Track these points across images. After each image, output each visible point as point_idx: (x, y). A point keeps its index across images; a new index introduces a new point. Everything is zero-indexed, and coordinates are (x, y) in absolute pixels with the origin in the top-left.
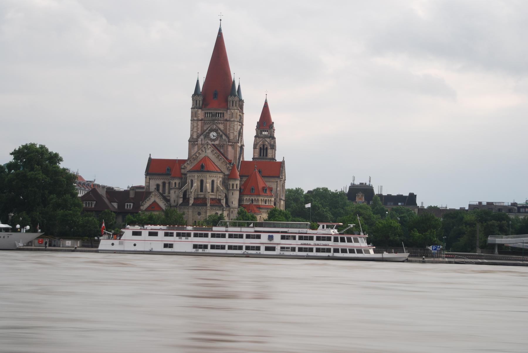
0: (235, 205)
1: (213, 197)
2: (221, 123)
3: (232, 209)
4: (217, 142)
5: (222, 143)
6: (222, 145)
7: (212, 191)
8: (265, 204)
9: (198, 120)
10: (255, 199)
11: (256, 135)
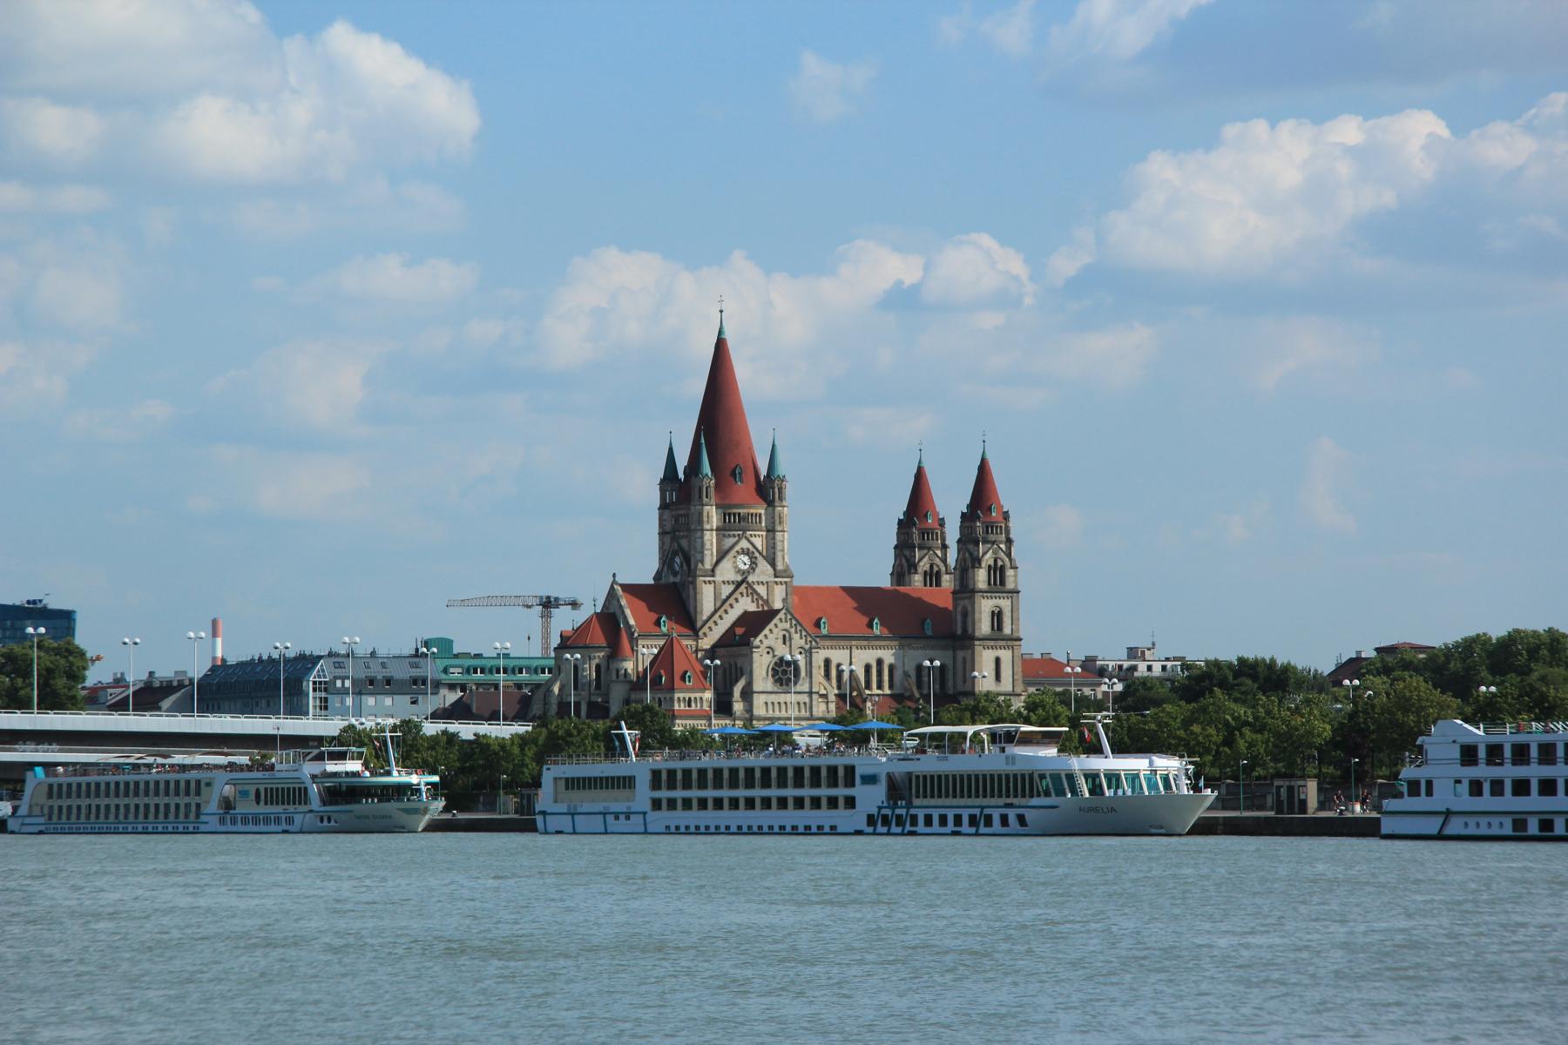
4: (678, 579)
11: (959, 536)
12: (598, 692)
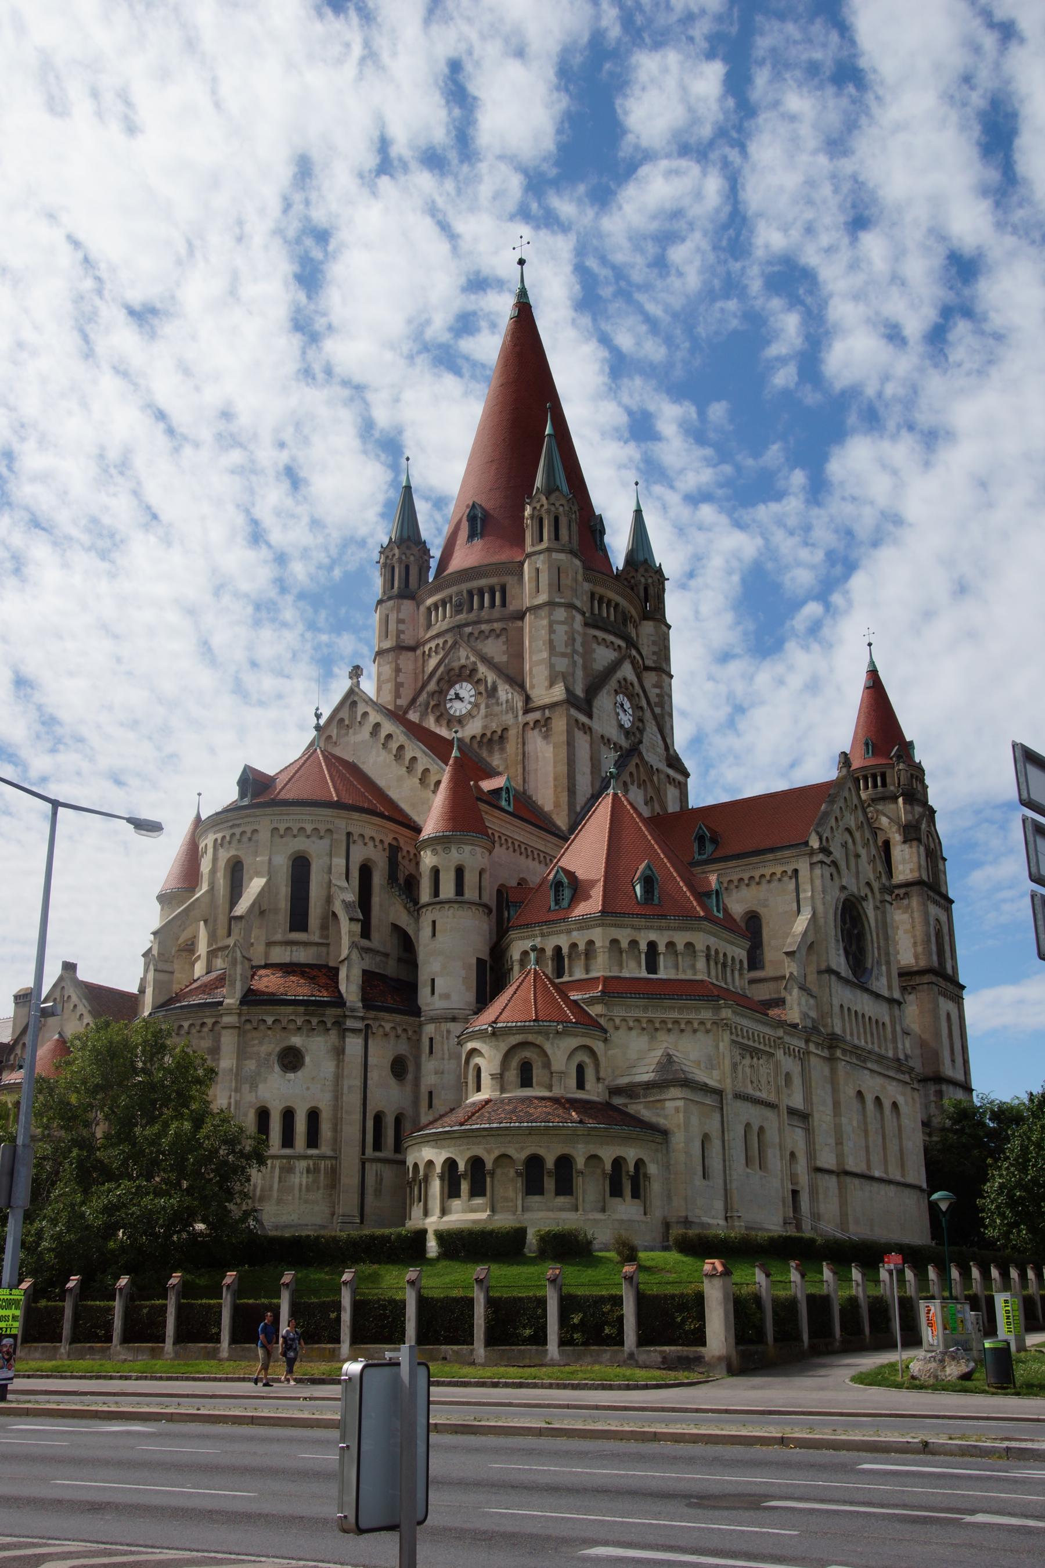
0: (446, 996)
1: (302, 956)
2: (493, 630)
3: (429, 1029)
4: (473, 728)
5: (494, 726)
6: (496, 737)
7: (299, 920)
8: (644, 974)
9: (400, 648)
10: (574, 946)
12: (365, 943)
